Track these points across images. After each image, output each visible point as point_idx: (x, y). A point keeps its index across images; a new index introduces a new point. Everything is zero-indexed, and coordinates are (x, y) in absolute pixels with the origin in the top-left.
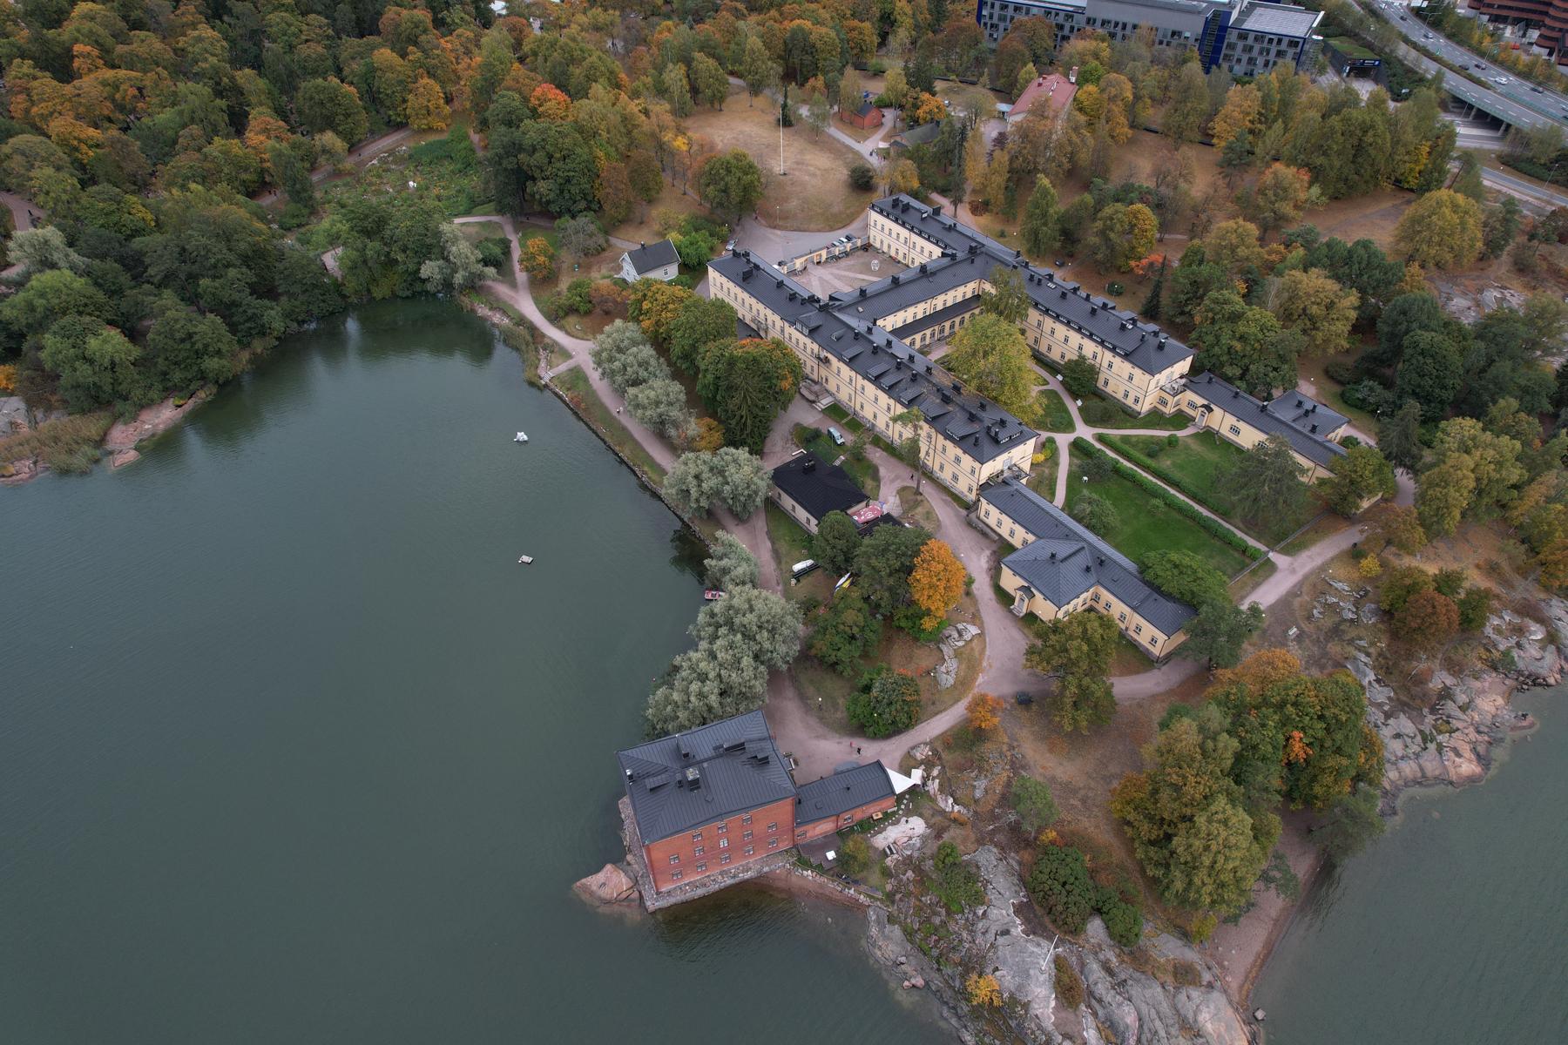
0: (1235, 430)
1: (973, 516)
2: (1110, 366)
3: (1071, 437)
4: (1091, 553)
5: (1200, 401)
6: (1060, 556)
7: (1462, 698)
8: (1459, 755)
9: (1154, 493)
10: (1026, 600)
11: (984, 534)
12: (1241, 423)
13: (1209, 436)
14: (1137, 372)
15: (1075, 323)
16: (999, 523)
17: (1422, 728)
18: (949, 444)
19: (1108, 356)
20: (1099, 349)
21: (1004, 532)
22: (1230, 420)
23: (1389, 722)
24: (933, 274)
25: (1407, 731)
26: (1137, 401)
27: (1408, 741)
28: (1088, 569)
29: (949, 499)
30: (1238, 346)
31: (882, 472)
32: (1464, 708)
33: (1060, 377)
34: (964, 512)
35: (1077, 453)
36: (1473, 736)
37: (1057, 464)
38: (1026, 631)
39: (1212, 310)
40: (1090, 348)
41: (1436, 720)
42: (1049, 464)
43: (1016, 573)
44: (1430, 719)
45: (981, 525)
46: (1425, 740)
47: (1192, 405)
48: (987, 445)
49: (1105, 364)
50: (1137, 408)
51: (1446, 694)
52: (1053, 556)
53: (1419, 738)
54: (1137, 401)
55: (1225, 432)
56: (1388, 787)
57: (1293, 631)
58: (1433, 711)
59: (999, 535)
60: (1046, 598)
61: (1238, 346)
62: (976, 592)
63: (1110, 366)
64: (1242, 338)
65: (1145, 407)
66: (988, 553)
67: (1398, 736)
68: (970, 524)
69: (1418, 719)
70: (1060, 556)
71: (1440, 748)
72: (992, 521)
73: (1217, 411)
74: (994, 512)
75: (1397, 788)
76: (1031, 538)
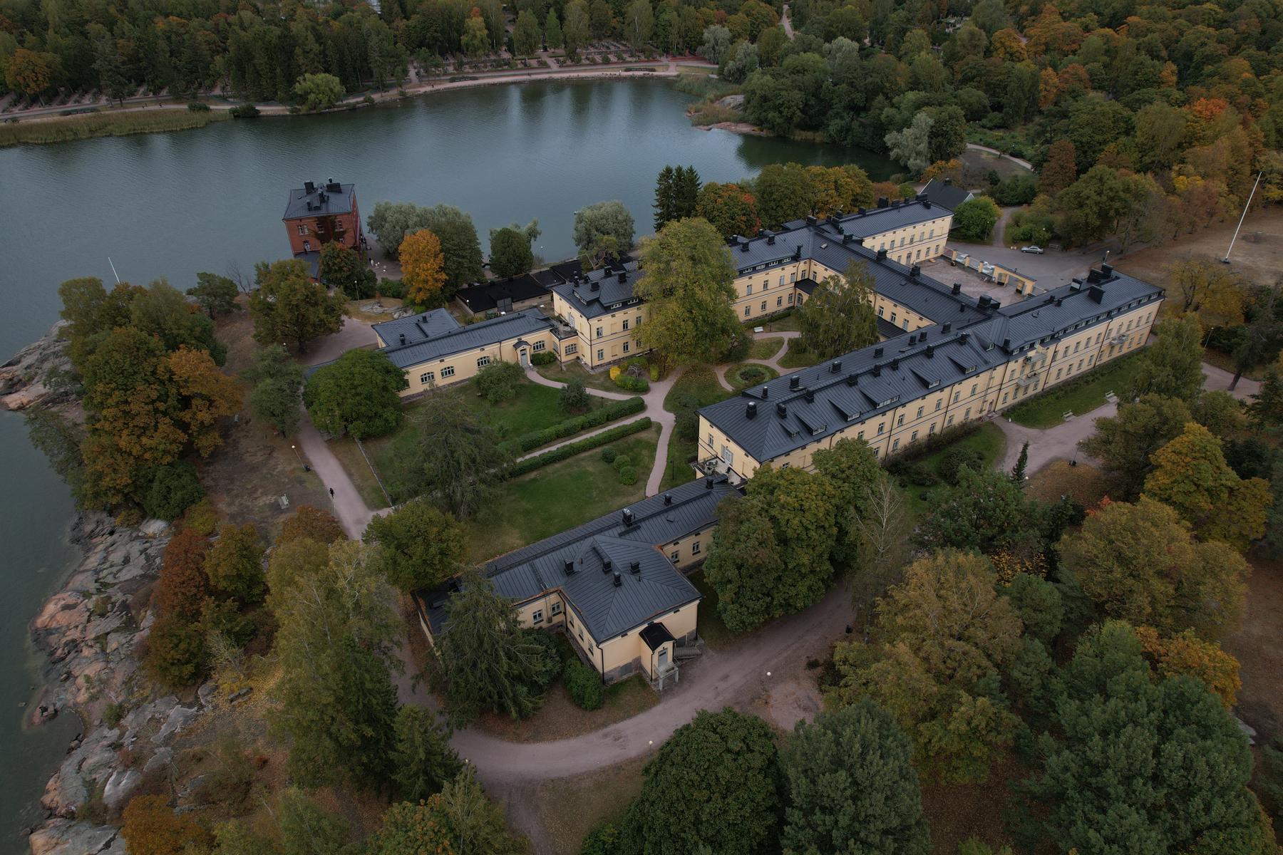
7: (114, 642)
8: (67, 607)
17: (116, 587)
23: (143, 556)
24: (916, 283)
25: (124, 572)
27: (114, 570)
32: (102, 639)
36: (74, 634)
41: (114, 604)
44: (119, 597)
46: (105, 585)
51: (130, 625)
53: (110, 579)
56: (94, 540)
57: (284, 501)
58: (125, 606)
67: (126, 561)
69: (128, 587)
71: (86, 595)
75: (89, 550)
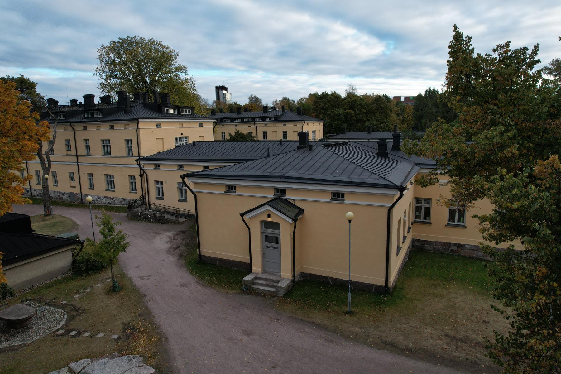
19: (261, 128)
38: (320, 317)
62: (137, 282)
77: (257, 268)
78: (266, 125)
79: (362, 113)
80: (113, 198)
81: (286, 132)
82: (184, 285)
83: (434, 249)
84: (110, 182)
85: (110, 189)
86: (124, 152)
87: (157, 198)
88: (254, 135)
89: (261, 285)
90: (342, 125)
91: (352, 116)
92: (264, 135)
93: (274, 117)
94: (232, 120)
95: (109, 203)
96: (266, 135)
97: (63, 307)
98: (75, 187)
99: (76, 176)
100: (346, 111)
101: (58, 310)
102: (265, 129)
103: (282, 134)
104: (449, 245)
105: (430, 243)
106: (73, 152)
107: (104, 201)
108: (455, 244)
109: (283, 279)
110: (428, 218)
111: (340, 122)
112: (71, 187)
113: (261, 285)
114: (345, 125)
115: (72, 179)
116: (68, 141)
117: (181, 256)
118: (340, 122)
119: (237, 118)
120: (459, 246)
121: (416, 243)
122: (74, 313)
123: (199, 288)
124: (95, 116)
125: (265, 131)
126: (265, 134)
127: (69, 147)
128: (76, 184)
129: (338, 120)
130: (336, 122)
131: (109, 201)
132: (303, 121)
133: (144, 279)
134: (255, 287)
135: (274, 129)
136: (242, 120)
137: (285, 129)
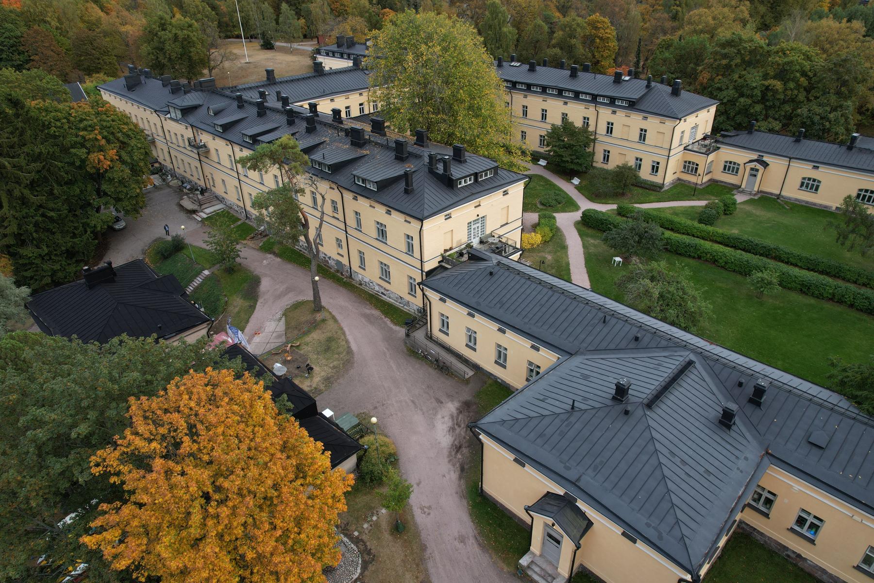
0: (810, 185)
1: (419, 335)
2: (610, 130)
3: (577, 216)
4: (715, 375)
5: (740, 156)
6: (641, 390)
9: (744, 270)
10: (568, 545)
11: (443, 368)
12: (823, 169)
13: (766, 200)
14: (653, 124)
15: (553, 88)
16: (472, 340)
18: (363, 204)
19: (605, 114)
20: (590, 112)
21: (485, 358)
22: (802, 170)
26: (655, 169)
28: (726, 420)
29: (377, 313)
30: (778, 85)
31: (265, 285)
33: (543, 162)
34: (401, 331)
35: (590, 231)
37: (564, 248)
39: (725, 56)
40: (577, 113)
42: (550, 248)
43: (522, 458)
45: (434, 350)
47: (730, 167)
48: (430, 192)
49: (602, 129)
50: (657, 179)
52: (621, 392)
54: (655, 169)
55: (792, 192)
59: (476, 367)
60: (632, 534)
61: (778, 85)
62: (420, 518)
63: (610, 130)
64: (783, 74)
65: (670, 175)
66: (452, 407)
68: (414, 353)
70: (641, 390)
72: (456, 340)
73: (776, 164)
74: (456, 313)
76: (546, 358)
77: (536, 545)
78: (614, 112)
79: (799, 86)
80: (387, 290)
81: (646, 131)
82: (462, 539)
83: (765, 541)
84: (386, 273)
85: (384, 277)
86: (404, 248)
87: (440, 330)
88: (591, 128)
89: (536, 572)
90: (754, 107)
91: (776, 92)
92: (608, 127)
93: (630, 101)
94: (560, 93)
95: (382, 293)
96: (612, 128)
97: (356, 541)
98: (343, 256)
99: (344, 244)
100: (766, 83)
101: (352, 545)
102: (612, 118)
103: (639, 131)
104: (786, 548)
105: (762, 534)
106: (340, 216)
107: (377, 288)
108: (794, 552)
109: (559, 574)
110: (768, 506)
111: (749, 101)
112: (338, 254)
113: (536, 572)
114: (758, 108)
115: (340, 246)
116: (333, 202)
117: (462, 469)
118: (749, 101)
119: (569, 91)
120: (799, 556)
121: (743, 525)
122: (367, 558)
123: (476, 549)
124: (368, 186)
125: (611, 121)
126: (607, 153)
127: (335, 209)
128: (344, 251)
129: (748, 97)
130: (742, 100)
131: (383, 291)
132: (678, 119)
133: (425, 513)
134: (530, 573)
135: (627, 121)
136: (577, 95)
137: (644, 125)
